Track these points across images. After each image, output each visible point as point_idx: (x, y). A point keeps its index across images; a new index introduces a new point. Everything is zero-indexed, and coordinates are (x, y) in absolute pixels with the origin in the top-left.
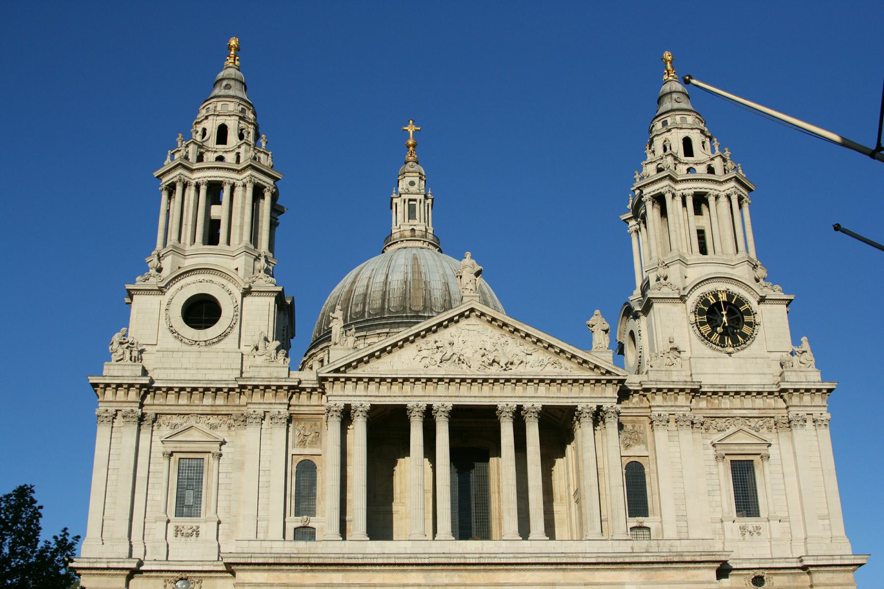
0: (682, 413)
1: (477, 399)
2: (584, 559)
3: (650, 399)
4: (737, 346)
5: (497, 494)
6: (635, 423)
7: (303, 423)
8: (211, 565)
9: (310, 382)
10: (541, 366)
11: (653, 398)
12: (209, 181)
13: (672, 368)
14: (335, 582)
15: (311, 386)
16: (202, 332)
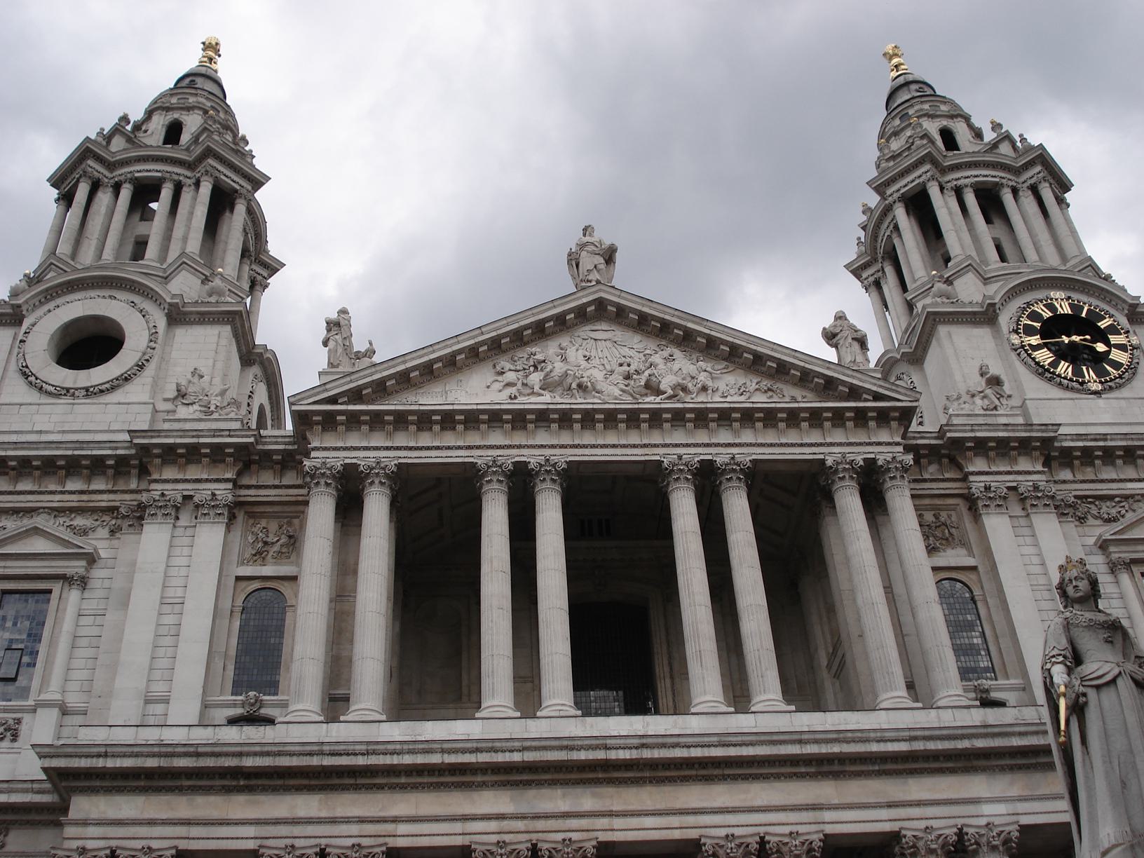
0: (1031, 484)
1: (618, 451)
2: (882, 744)
3: (963, 462)
4: (1107, 382)
5: (668, 681)
6: (940, 510)
7: (264, 523)
8: (26, 791)
9: (280, 440)
10: (742, 394)
11: (971, 460)
12: (136, 178)
13: (994, 412)
14: (302, 813)
15: (281, 447)
16: (83, 374)
